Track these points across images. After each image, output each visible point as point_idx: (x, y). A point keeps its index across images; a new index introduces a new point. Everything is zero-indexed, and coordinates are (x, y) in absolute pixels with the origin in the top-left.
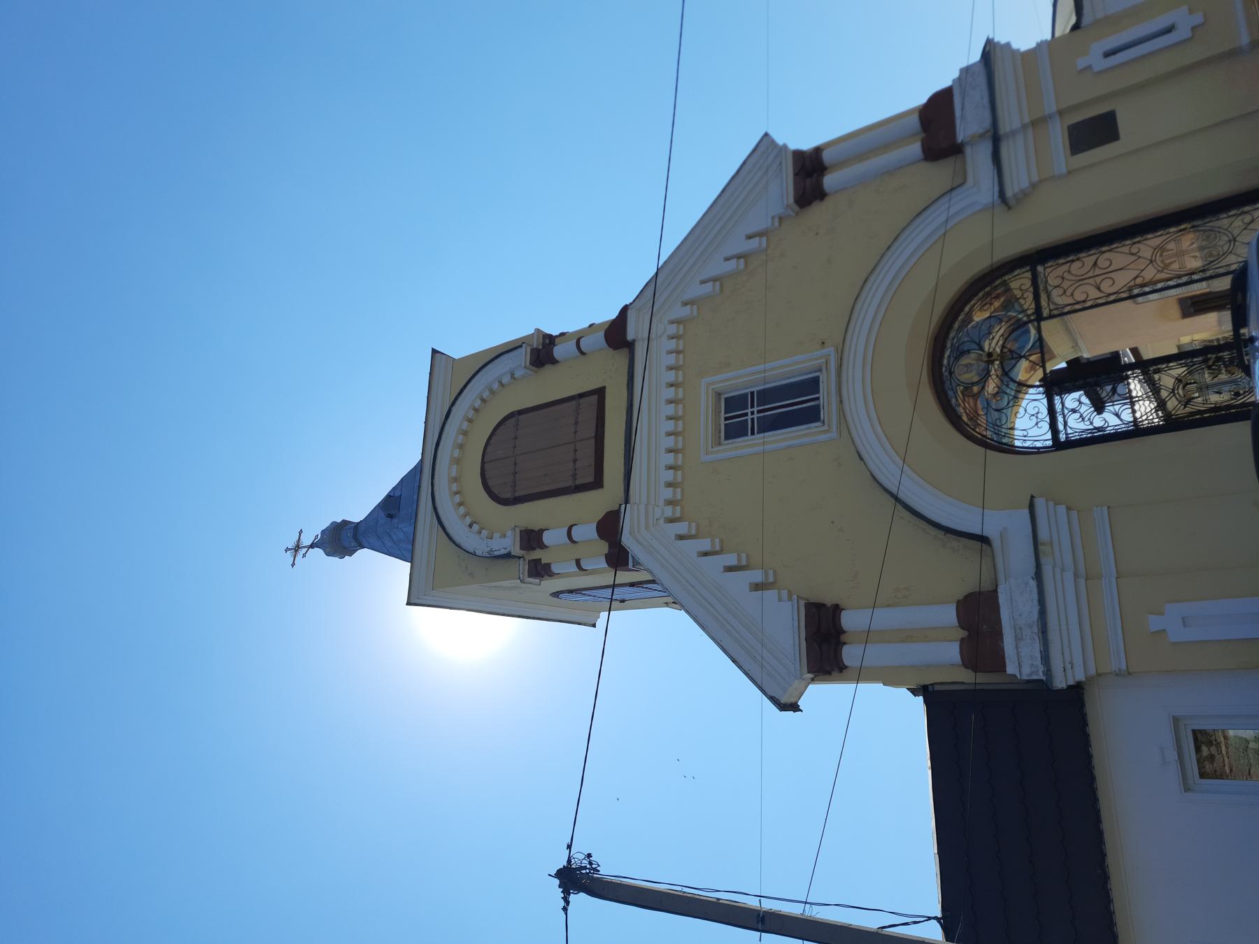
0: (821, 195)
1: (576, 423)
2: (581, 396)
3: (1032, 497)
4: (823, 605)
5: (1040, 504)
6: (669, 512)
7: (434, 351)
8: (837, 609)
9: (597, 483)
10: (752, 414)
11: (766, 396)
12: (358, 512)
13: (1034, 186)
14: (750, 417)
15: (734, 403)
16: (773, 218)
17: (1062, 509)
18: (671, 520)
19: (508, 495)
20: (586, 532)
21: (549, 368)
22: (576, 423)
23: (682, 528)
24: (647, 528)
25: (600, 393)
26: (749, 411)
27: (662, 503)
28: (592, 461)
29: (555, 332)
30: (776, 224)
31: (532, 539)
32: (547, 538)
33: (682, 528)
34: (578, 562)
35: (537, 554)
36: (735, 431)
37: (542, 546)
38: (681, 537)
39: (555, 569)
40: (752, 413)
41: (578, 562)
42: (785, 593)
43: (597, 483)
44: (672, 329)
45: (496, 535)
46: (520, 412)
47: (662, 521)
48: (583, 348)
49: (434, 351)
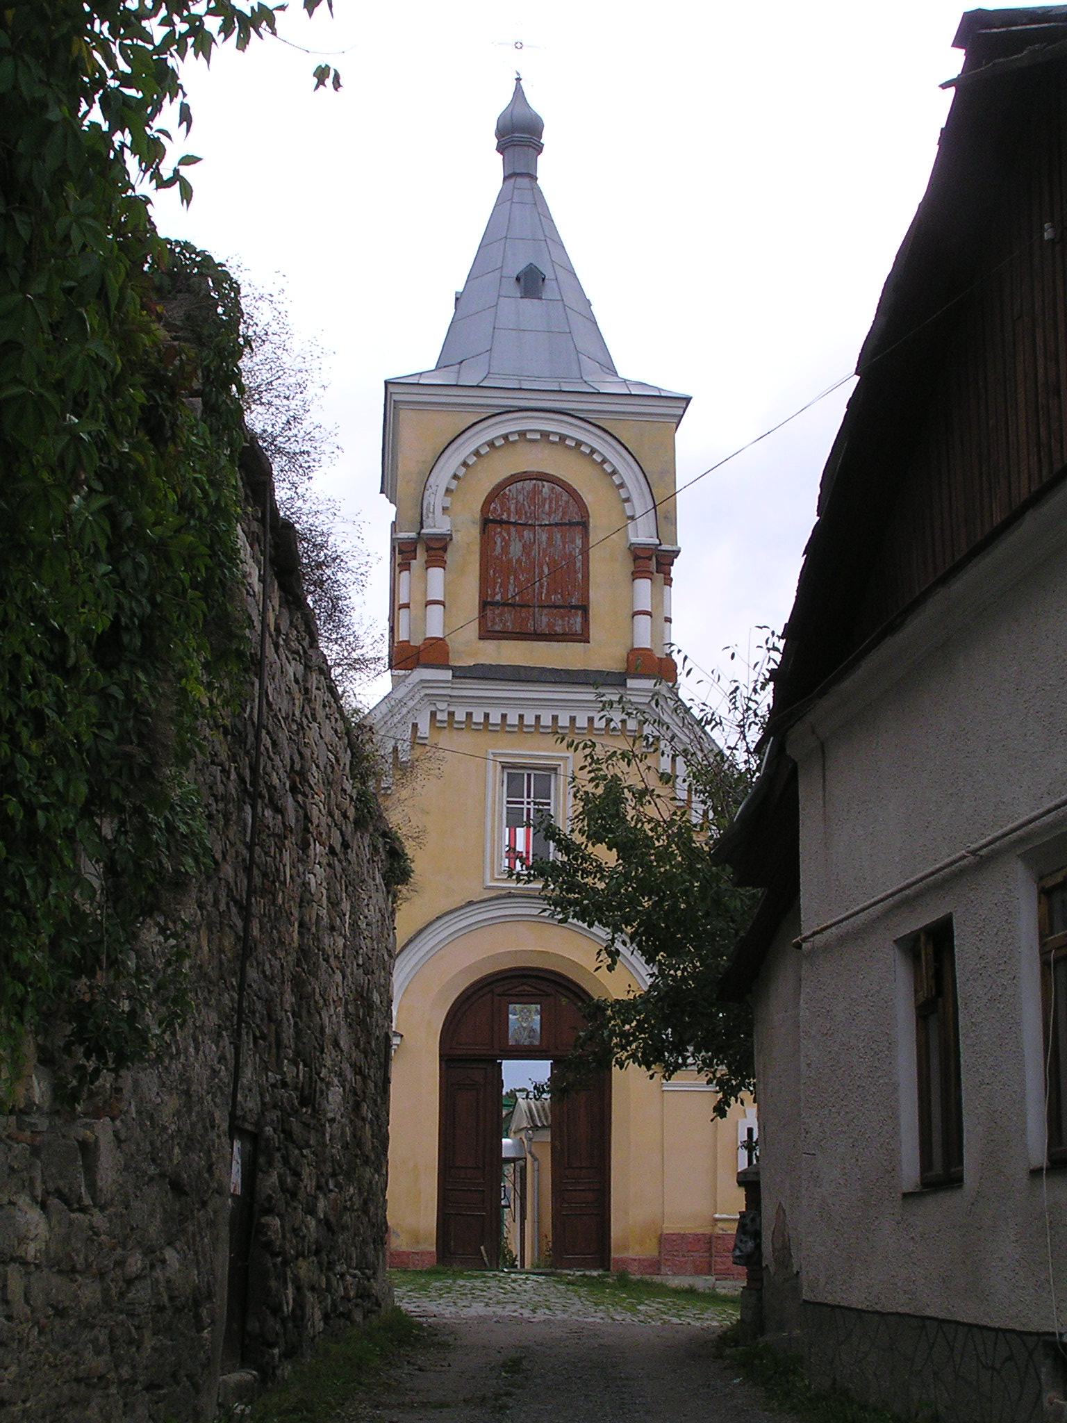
7: (688, 400)
9: (486, 634)
12: (550, 170)
14: (526, 800)
18: (433, 714)
20: (435, 626)
23: (424, 729)
25: (583, 637)
27: (452, 709)
29: (675, 571)
32: (436, 574)
33: (424, 729)
34: (407, 606)
35: (421, 555)
37: (429, 564)
38: (415, 726)
39: (405, 574)
41: (407, 606)
43: (486, 634)
45: (448, 502)
49: (688, 400)
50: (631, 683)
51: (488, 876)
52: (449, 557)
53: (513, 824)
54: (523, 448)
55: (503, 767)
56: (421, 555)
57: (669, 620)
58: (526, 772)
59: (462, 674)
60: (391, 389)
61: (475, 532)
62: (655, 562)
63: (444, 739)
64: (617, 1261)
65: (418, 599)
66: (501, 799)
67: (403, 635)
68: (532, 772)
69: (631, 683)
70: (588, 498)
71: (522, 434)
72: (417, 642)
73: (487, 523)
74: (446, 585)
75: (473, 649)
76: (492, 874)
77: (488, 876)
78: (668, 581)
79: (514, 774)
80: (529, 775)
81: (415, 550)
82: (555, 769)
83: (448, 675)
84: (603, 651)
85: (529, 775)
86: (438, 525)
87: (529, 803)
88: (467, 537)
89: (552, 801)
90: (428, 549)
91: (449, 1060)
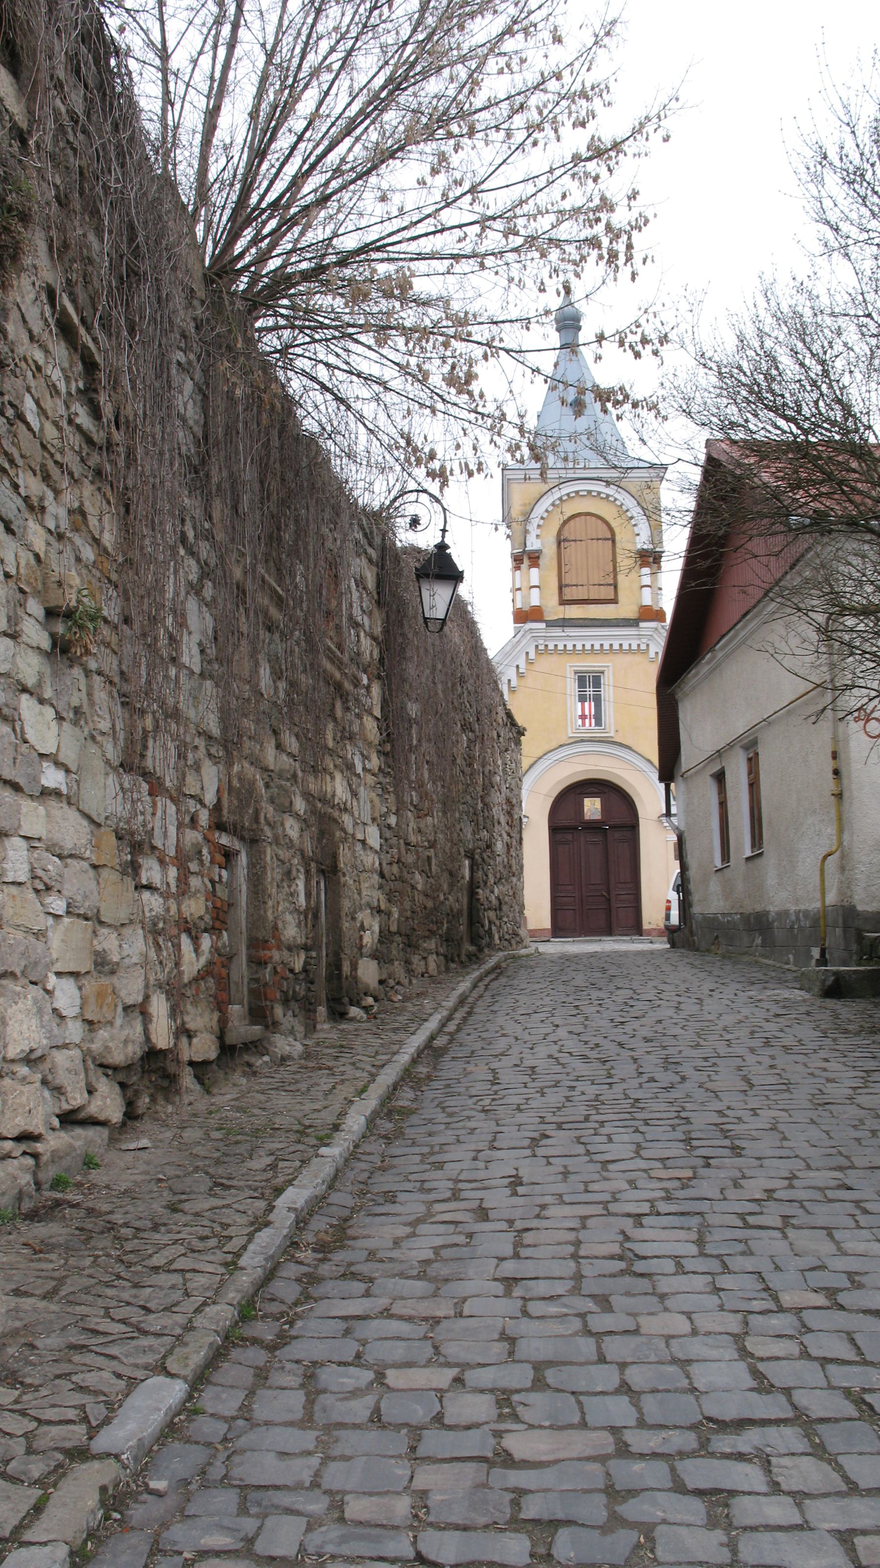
2: (616, 587)
6: (541, 647)
9: (563, 602)
10: (590, 691)
15: (597, 682)
23: (532, 655)
25: (614, 601)
31: (534, 558)
32: (534, 571)
33: (532, 655)
35: (526, 562)
36: (582, 681)
37: (531, 567)
43: (563, 602)
44: (643, 647)
45: (538, 532)
46: (614, 541)
52: (541, 562)
53: (582, 699)
54: (578, 500)
56: (526, 562)
59: (551, 624)
61: (554, 547)
67: (519, 606)
69: (642, 624)
71: (577, 492)
72: (526, 608)
73: (560, 541)
74: (541, 578)
75: (555, 611)
78: (659, 568)
84: (626, 609)
86: (533, 544)
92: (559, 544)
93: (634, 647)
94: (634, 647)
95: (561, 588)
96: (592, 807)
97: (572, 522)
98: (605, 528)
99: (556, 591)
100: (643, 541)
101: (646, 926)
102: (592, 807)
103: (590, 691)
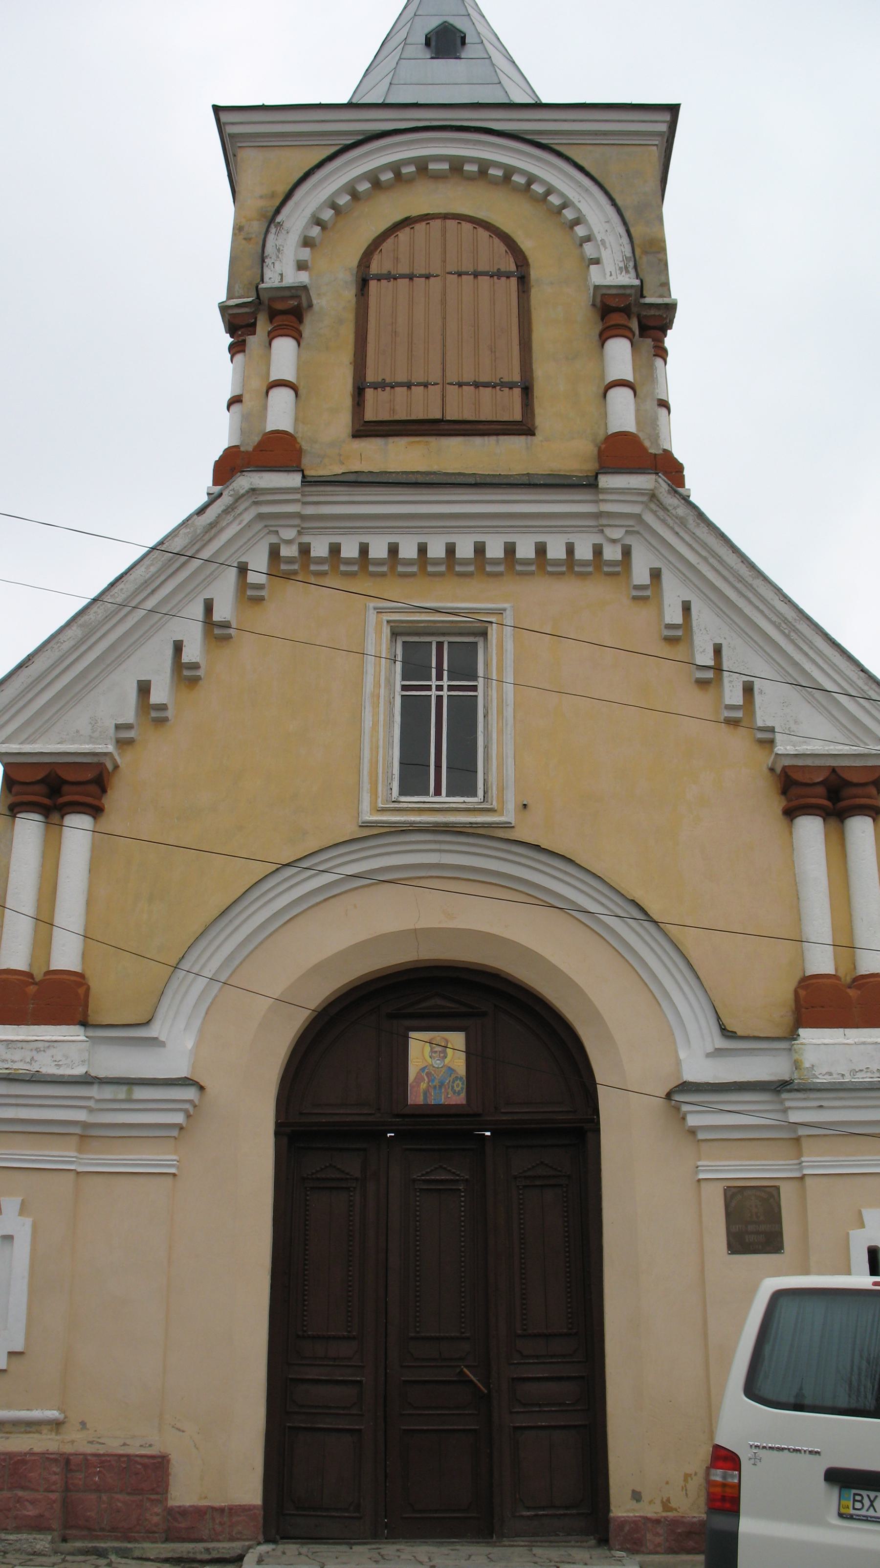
0: (791, 813)
1: (477, 385)
2: (527, 391)
3: (202, 1088)
4: (104, 791)
5: (190, 1093)
6: (287, 551)
8: (96, 811)
11: (464, 715)
13: (693, 1131)
16: (772, 730)
17: (178, 1118)
18: (274, 553)
19: (374, 269)
20: (280, 413)
21: (599, 327)
22: (477, 385)
24: (261, 517)
25: (524, 428)
26: (445, 683)
27: (305, 539)
28: (401, 415)
29: (671, 340)
30: (760, 735)
32: (284, 347)
35: (263, 326)
37: (271, 336)
38: (243, 569)
39: (239, 357)
40: (439, 688)
42: (131, 734)
44: (612, 553)
45: (305, 254)
46: (523, 281)
47: (274, 539)
48: (613, 393)
50: (605, 481)
51: (366, 805)
52: (307, 330)
55: (395, 634)
56: (263, 326)
57: (664, 404)
58: (434, 640)
60: (224, 117)
61: (349, 294)
62: (640, 317)
63: (292, 591)
64: (623, 1522)
65: (258, 384)
66: (390, 684)
68: (446, 640)
69: (605, 481)
70: (526, 244)
74: (301, 367)
76: (374, 802)
77: (366, 805)
78: (661, 353)
79: (417, 648)
80: (440, 645)
81: (254, 325)
82: (484, 634)
83: (294, 480)
85: (440, 645)
86: (282, 272)
87: (439, 688)
88: (332, 299)
89: (480, 683)
90: (273, 315)
91: (301, 1137)
92: (363, 283)
93: (584, 552)
94: (584, 552)
95: (359, 393)
96: (436, 1062)
97: (404, 235)
98: (500, 247)
99: (347, 402)
100: (612, 272)
101: (621, 1508)
102: (436, 1062)
103: (439, 688)
